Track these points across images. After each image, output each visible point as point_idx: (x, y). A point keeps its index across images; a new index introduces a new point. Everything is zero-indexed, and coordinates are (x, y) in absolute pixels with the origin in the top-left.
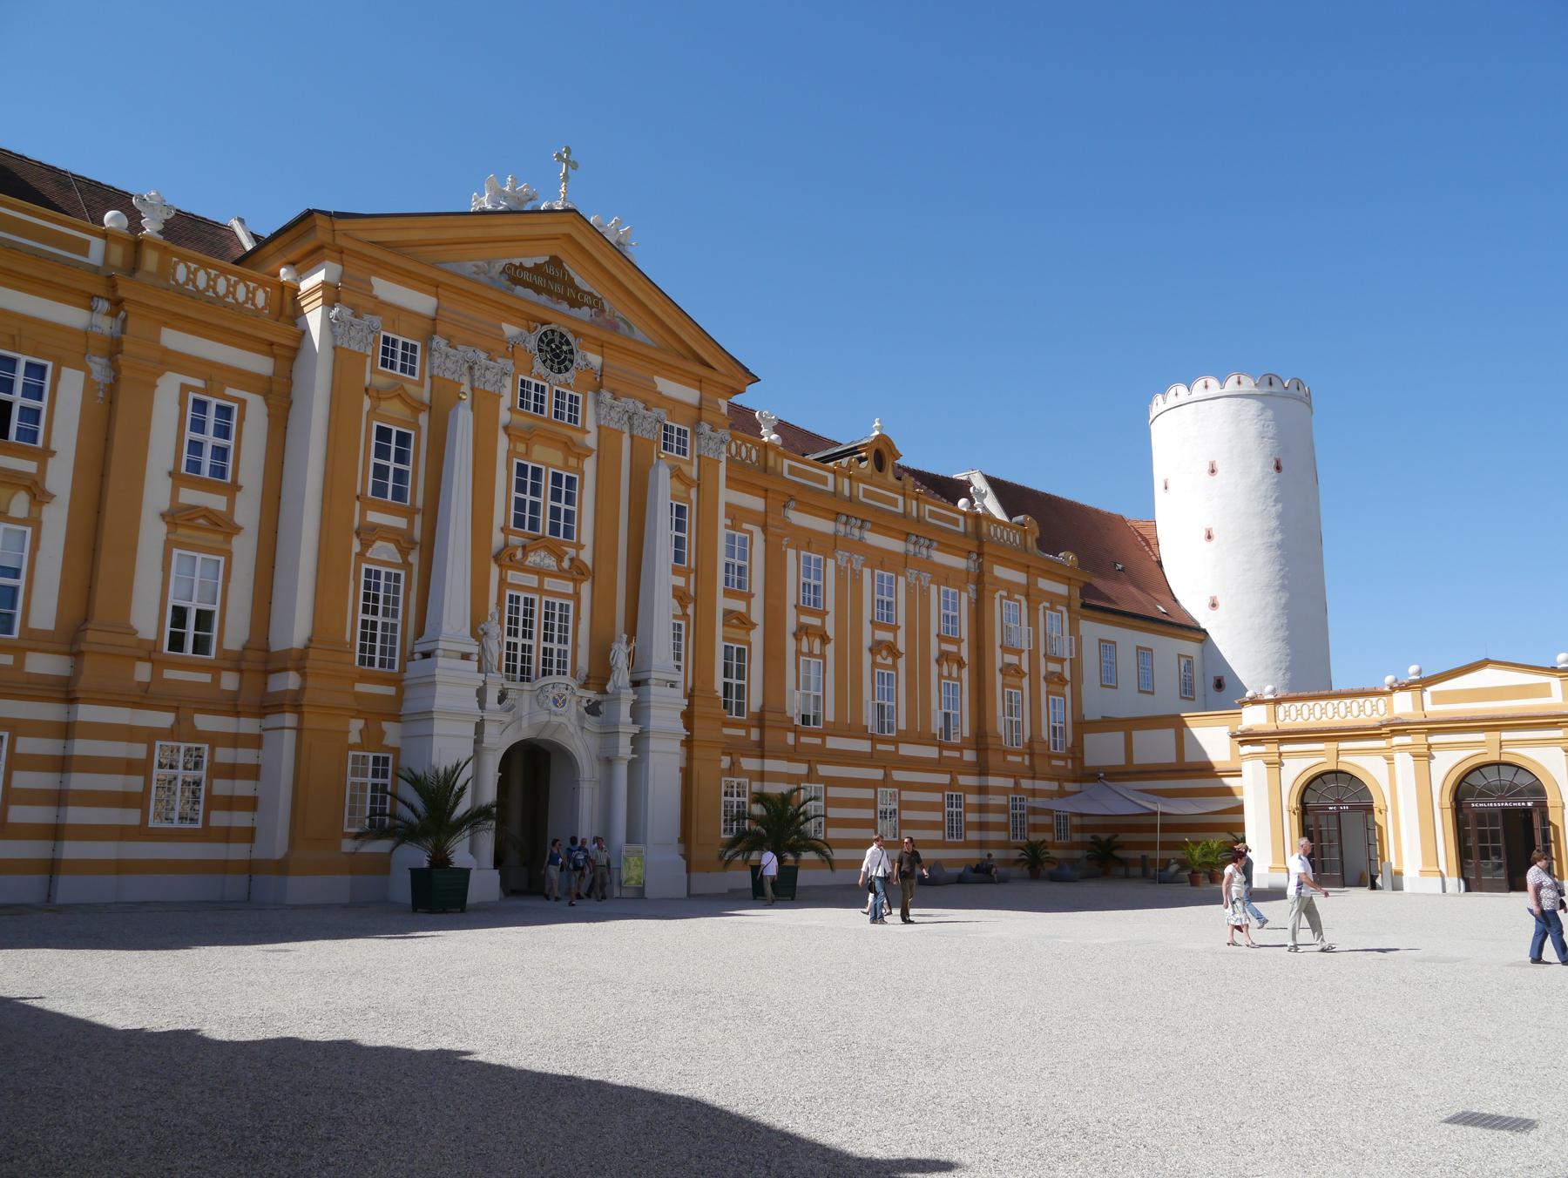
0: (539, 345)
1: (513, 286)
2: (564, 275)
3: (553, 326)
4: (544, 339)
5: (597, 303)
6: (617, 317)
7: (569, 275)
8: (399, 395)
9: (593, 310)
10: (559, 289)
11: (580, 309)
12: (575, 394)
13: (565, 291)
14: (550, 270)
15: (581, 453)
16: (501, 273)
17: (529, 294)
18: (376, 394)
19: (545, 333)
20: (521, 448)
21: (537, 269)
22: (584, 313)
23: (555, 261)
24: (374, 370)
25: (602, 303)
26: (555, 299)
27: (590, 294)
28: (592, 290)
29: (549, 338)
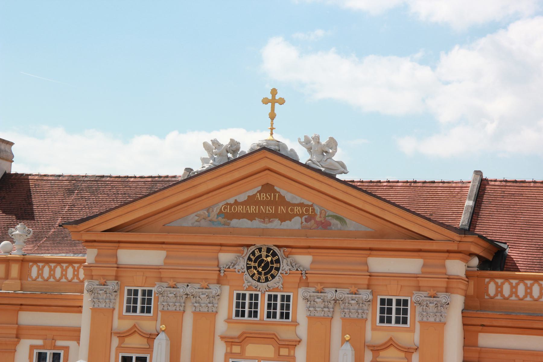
0: (247, 264)
1: (229, 221)
2: (275, 196)
3: (258, 245)
4: (252, 257)
5: (307, 211)
6: (328, 216)
7: (280, 196)
8: (135, 331)
9: (303, 218)
10: (270, 210)
11: (291, 221)
12: (286, 294)
13: (276, 210)
14: (263, 197)
15: (293, 344)
16: (219, 214)
17: (245, 223)
18: (122, 336)
19: (253, 253)
20: (236, 349)
21: (251, 200)
22: (295, 223)
23: (268, 188)
24: (121, 317)
25: (313, 210)
26: (267, 220)
27: (301, 205)
28: (303, 201)
29: (256, 255)
